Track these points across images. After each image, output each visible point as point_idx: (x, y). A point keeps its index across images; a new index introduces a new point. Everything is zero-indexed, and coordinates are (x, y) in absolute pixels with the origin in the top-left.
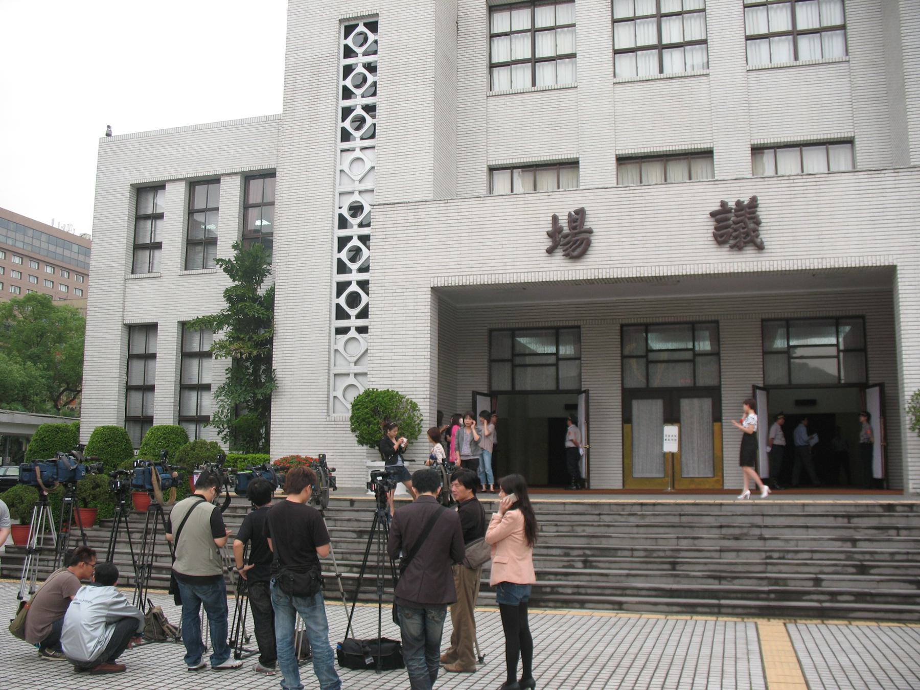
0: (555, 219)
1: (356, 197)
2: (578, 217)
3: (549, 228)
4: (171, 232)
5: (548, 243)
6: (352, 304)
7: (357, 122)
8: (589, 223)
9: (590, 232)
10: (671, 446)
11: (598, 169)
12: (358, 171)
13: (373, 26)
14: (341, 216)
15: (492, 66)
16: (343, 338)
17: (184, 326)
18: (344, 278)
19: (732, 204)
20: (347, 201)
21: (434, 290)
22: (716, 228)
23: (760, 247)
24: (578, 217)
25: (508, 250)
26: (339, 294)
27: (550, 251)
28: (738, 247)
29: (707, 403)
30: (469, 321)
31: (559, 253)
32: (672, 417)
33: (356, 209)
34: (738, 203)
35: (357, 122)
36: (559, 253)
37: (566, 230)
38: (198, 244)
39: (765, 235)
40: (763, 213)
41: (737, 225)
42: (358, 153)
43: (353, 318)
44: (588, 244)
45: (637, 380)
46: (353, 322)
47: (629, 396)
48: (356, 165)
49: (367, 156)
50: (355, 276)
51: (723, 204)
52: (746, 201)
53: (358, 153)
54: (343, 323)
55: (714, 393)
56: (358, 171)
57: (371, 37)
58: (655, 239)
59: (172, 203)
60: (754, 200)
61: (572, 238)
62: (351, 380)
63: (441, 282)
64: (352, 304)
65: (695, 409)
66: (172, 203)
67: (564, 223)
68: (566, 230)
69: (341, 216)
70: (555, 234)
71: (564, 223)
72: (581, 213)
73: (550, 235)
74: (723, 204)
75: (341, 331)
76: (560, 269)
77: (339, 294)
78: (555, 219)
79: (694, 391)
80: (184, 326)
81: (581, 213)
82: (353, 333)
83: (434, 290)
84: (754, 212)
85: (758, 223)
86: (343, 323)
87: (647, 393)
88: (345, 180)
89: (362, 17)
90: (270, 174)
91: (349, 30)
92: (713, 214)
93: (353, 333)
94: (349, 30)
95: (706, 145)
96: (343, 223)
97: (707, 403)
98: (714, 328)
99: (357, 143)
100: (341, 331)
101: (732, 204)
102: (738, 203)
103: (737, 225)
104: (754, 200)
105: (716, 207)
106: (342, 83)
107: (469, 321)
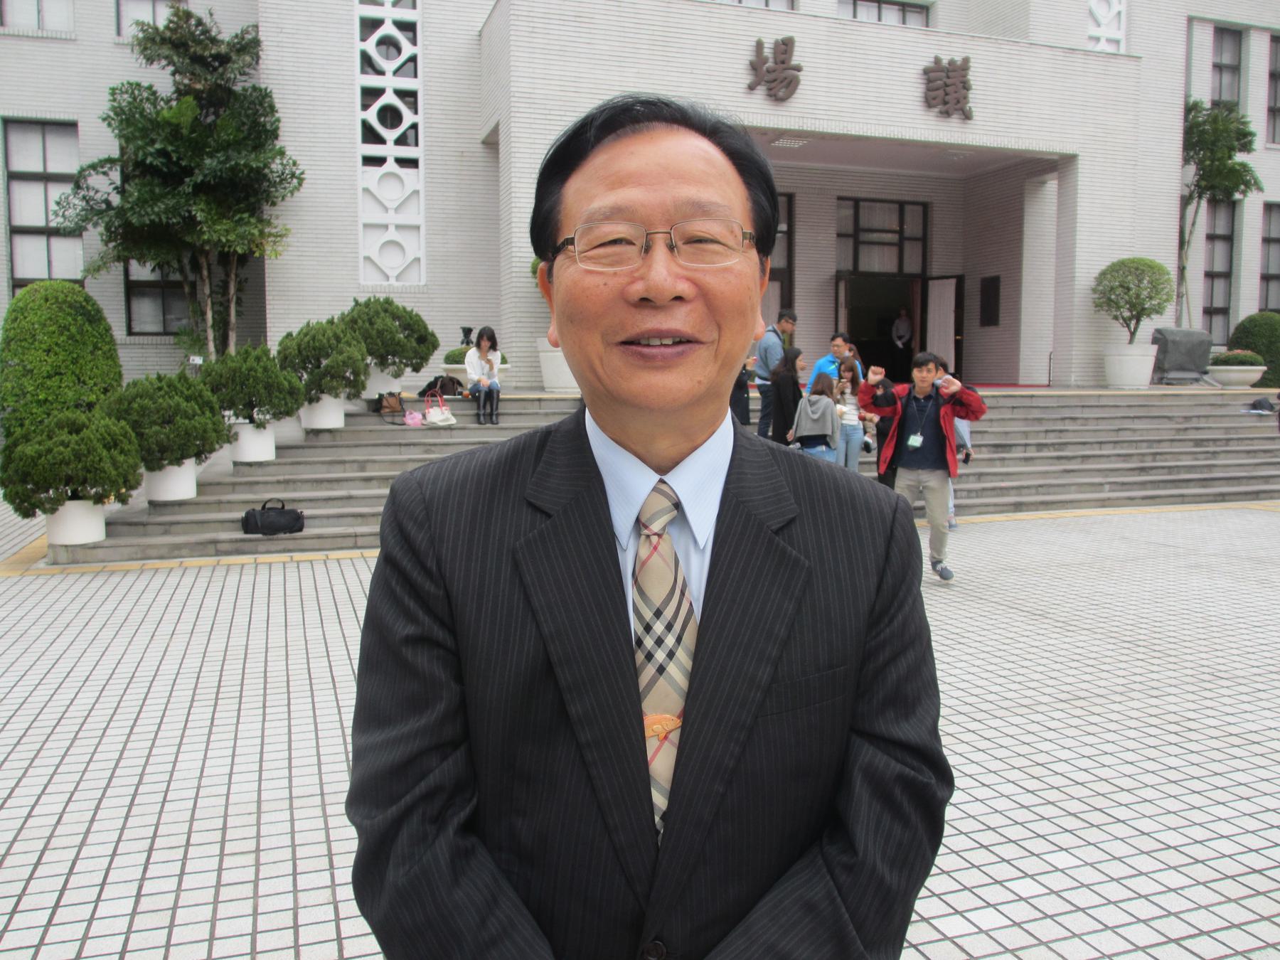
0: (759, 45)
2: (785, 46)
5: (747, 78)
9: (798, 69)
18: (373, 81)
19: (945, 62)
22: (928, 90)
23: (967, 116)
24: (785, 46)
26: (365, 107)
27: (751, 88)
28: (946, 114)
31: (761, 91)
36: (761, 91)
40: (972, 77)
41: (946, 88)
43: (390, 143)
50: (390, 82)
51: (937, 61)
52: (958, 59)
54: (374, 150)
60: (966, 61)
67: (768, 52)
68: (770, 64)
70: (755, 67)
71: (768, 52)
74: (937, 61)
75: (370, 161)
77: (365, 107)
78: (759, 45)
82: (391, 166)
84: (965, 76)
85: (966, 86)
86: (374, 150)
92: (926, 72)
93: (391, 166)
101: (945, 62)
104: (966, 61)
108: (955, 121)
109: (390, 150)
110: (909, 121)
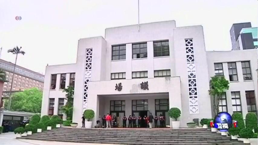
0: (117, 84)
3: (116, 85)
5: (115, 88)
7: (89, 66)
8: (122, 85)
9: (122, 86)
12: (88, 74)
13: (91, 50)
14: (85, 82)
16: (85, 102)
19: (144, 82)
20: (86, 79)
21: (98, 95)
23: (148, 89)
25: (109, 89)
27: (116, 89)
28: (145, 89)
29: (123, 113)
31: (117, 90)
34: (145, 82)
35: (89, 66)
37: (118, 86)
38: (62, 86)
39: (149, 88)
40: (149, 84)
41: (145, 86)
42: (88, 71)
44: (122, 88)
48: (88, 73)
49: (90, 72)
51: (143, 82)
52: (146, 82)
54: (85, 100)
56: (88, 74)
57: (91, 52)
60: (147, 82)
61: (119, 87)
67: (118, 85)
68: (118, 86)
69: (85, 82)
71: (118, 85)
72: (121, 83)
73: (116, 87)
74: (143, 82)
76: (117, 92)
78: (117, 84)
81: (121, 83)
83: (98, 95)
85: (148, 85)
86: (85, 100)
89: (90, 49)
90: (75, 73)
91: (88, 50)
92: (141, 84)
95: (147, 70)
96: (86, 83)
97: (123, 113)
98: (147, 100)
99: (88, 69)
101: (144, 82)
102: (145, 82)
104: (147, 82)
105: (141, 83)
106: (86, 59)
108: (147, 90)
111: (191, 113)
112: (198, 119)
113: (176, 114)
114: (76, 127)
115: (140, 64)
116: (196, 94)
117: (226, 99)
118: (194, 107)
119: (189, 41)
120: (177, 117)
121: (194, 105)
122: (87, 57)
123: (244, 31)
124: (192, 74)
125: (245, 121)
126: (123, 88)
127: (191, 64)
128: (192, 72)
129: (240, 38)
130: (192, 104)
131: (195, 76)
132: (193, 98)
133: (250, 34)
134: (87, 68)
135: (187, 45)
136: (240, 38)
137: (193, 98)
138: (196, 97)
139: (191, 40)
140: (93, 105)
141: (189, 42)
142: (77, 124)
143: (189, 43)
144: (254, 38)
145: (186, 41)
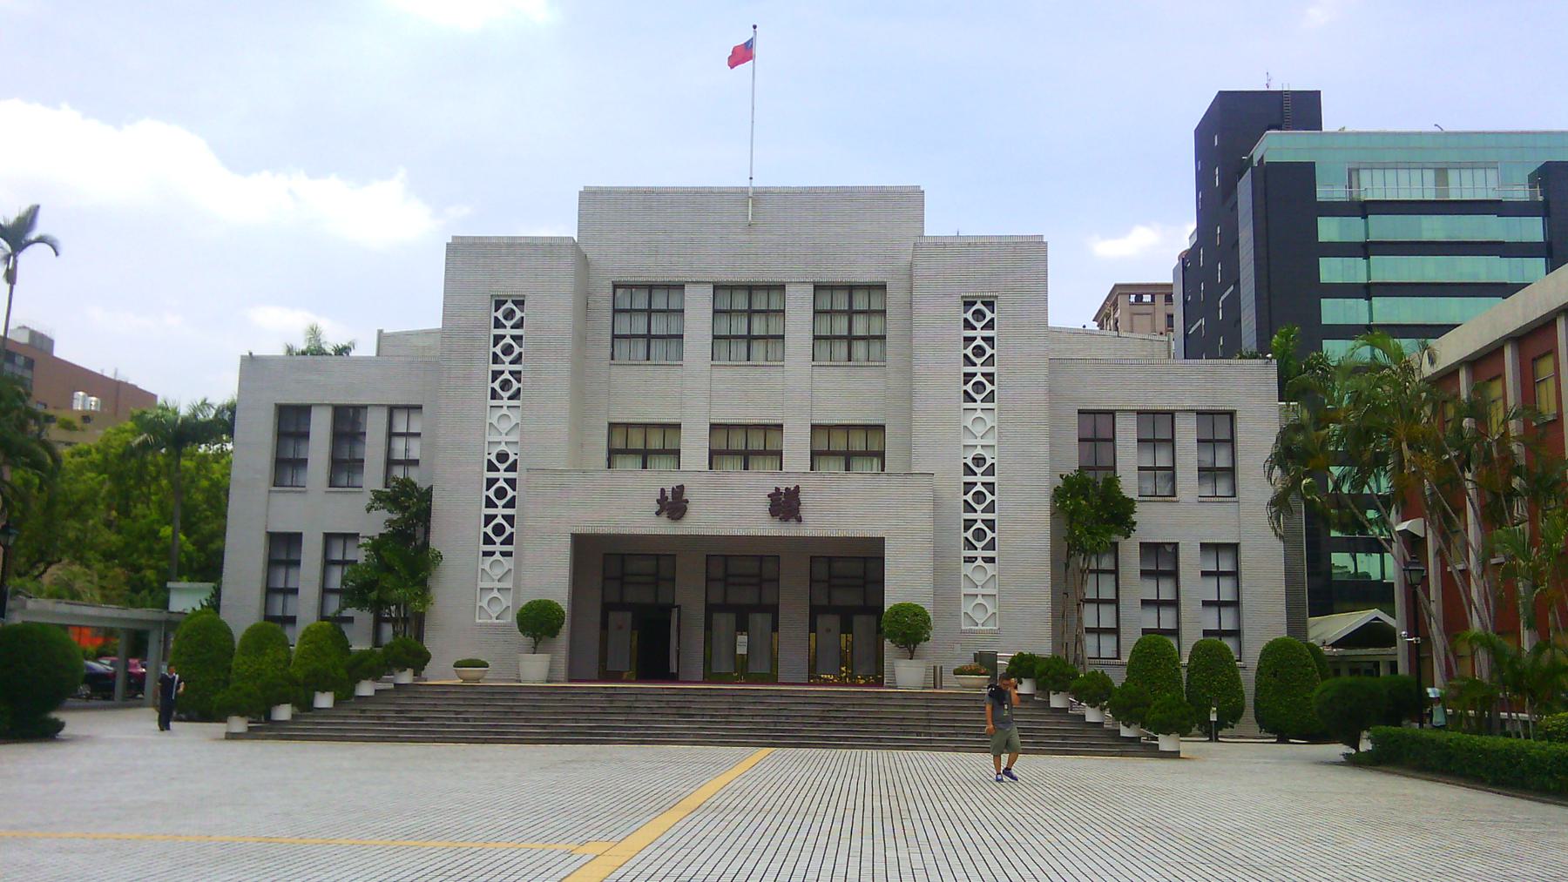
1: (503, 447)
4: (319, 447)
5: (657, 507)
6: (500, 534)
10: (742, 650)
11: (695, 448)
15: (614, 337)
17: (329, 537)
19: (783, 490)
23: (799, 520)
28: (785, 519)
30: (597, 557)
32: (742, 627)
33: (502, 457)
36: (664, 516)
38: (344, 466)
39: (803, 514)
40: (802, 497)
41: (785, 505)
45: (717, 597)
46: (498, 548)
47: (710, 609)
53: (505, 411)
54: (489, 548)
55: (774, 610)
56: (504, 426)
58: (730, 508)
59: (321, 427)
62: (495, 594)
63: (579, 531)
64: (500, 534)
65: (760, 621)
66: (321, 427)
67: (669, 494)
70: (662, 500)
71: (669, 494)
72: (681, 488)
75: (486, 554)
76: (663, 527)
79: (760, 608)
80: (329, 537)
81: (681, 488)
82: (497, 556)
86: (489, 548)
87: (724, 608)
88: (494, 432)
93: (497, 556)
94: (499, 304)
100: (486, 554)
101: (783, 490)
103: (785, 505)
107: (597, 557)
108: (793, 522)
109: (498, 548)
110: (760, 524)
111: (965, 626)
112: (994, 656)
113: (911, 630)
114: (478, 680)
115: (744, 394)
116: (991, 545)
117: (1115, 572)
118: (980, 600)
119: (979, 306)
120: (916, 643)
121: (979, 591)
122: (498, 339)
123: (1276, 146)
124: (979, 460)
125: (1184, 672)
126: (691, 508)
127: (979, 414)
128: (979, 451)
129: (1245, 186)
130: (973, 591)
131: (991, 471)
132: (979, 562)
133: (1305, 173)
134: (494, 395)
135: (968, 325)
136: (1245, 186)
137: (979, 562)
138: (992, 560)
139: (990, 304)
140: (551, 579)
141: (978, 308)
142: (485, 665)
143: (979, 315)
144: (1323, 193)
145: (968, 304)
